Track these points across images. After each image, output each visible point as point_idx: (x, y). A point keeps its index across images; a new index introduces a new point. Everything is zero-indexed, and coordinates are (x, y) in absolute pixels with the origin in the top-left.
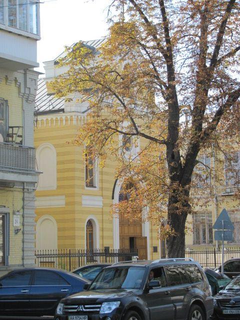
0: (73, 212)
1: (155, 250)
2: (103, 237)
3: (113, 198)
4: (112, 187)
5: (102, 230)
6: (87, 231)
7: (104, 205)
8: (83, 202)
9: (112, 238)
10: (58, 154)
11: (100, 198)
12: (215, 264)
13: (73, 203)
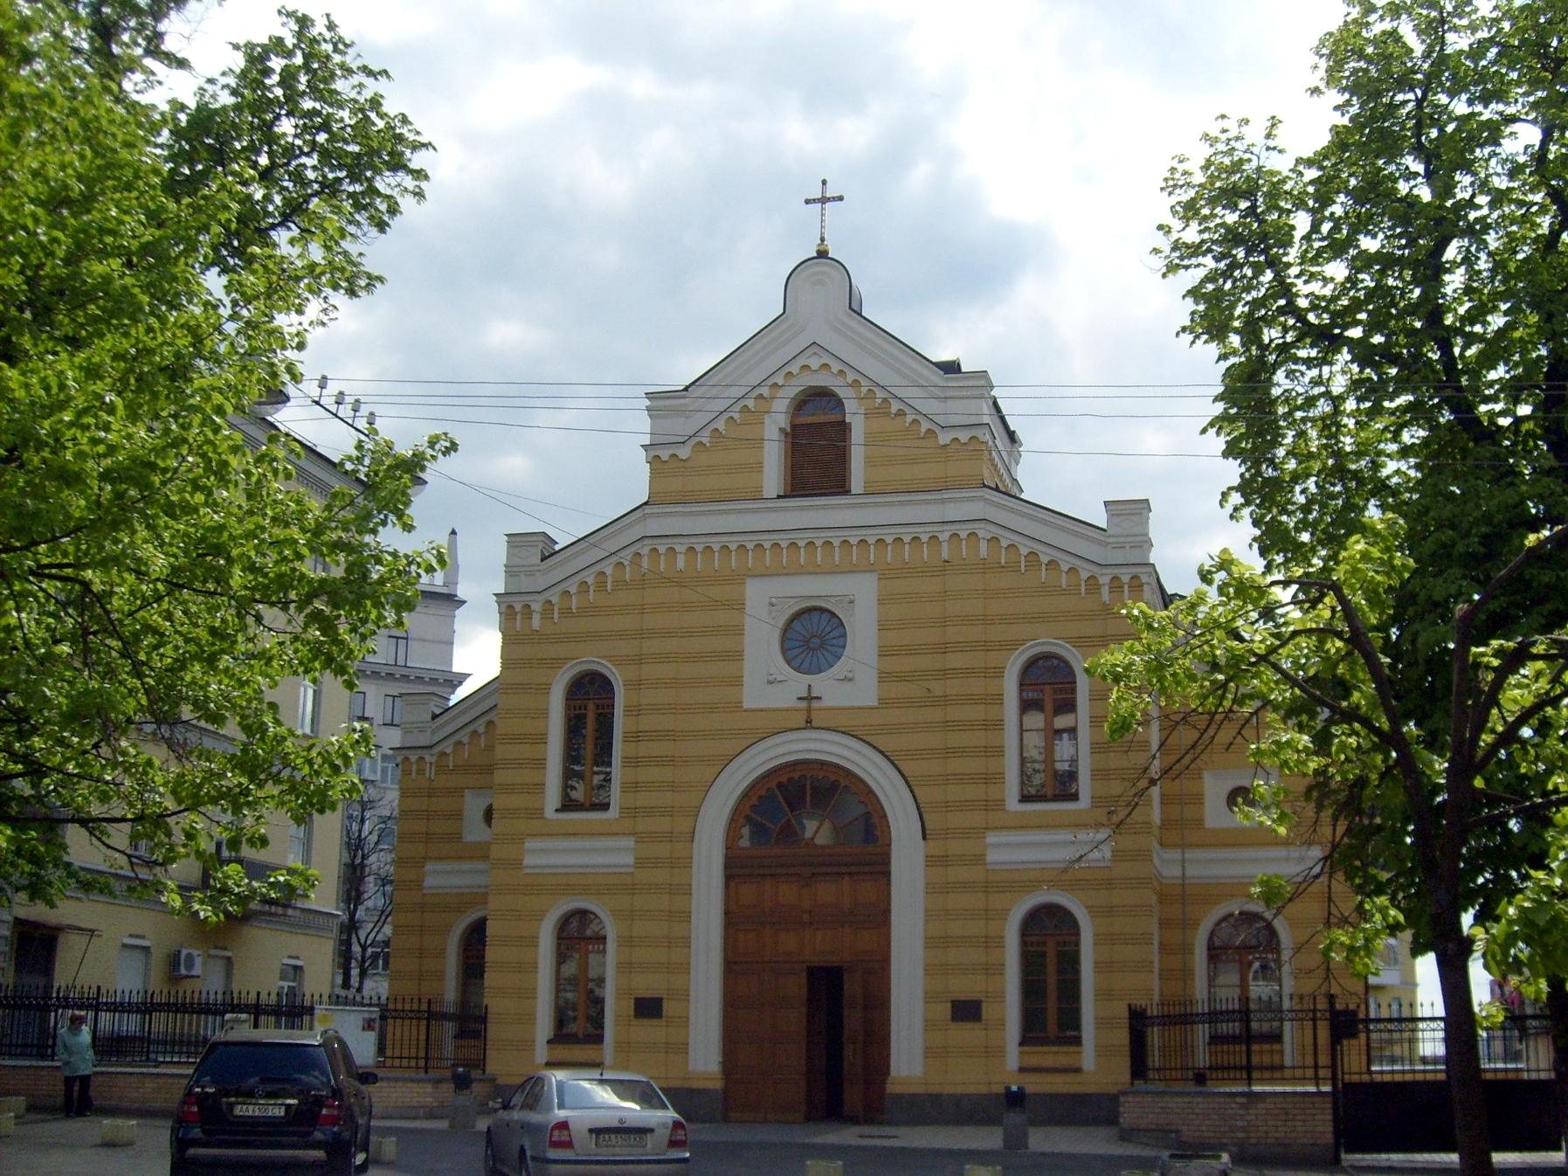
5: (627, 942)
7: (641, 863)
11: (629, 842)
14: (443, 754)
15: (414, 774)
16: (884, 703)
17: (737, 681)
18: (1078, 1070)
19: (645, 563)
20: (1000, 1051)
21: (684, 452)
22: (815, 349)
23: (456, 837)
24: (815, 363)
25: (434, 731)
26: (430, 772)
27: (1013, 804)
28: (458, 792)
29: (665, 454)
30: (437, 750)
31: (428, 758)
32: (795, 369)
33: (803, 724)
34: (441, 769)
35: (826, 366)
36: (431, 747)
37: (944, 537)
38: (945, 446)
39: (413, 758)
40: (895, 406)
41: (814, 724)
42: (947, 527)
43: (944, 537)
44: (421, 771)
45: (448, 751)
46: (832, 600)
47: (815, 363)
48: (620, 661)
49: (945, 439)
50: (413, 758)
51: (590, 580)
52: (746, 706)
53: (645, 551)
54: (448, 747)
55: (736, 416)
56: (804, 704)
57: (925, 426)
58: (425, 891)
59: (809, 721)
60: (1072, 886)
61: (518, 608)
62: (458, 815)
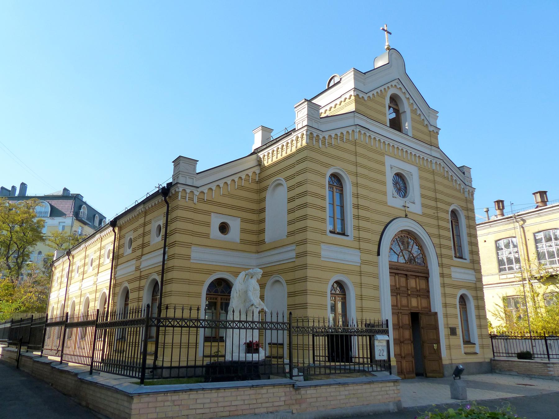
0: (304, 267)
1: (453, 331)
2: (361, 309)
3: (379, 254)
4: (378, 240)
7: (364, 262)
8: (323, 253)
9: (379, 311)
10: (290, 189)
11: (357, 252)
13: (304, 254)
14: (202, 192)
15: (187, 198)
16: (424, 215)
17: (385, 193)
18: (476, 353)
19: (357, 136)
20: (459, 346)
21: (366, 98)
22: (397, 81)
23: (207, 236)
24: (398, 87)
27: (454, 258)
28: (208, 213)
29: (361, 95)
30: (200, 190)
31: (197, 193)
32: (394, 83)
33: (405, 216)
35: (400, 88)
36: (198, 187)
37: (434, 161)
38: (430, 132)
40: (419, 112)
41: (408, 216)
42: (435, 159)
43: (434, 161)
44: (191, 199)
45: (206, 191)
46: (406, 172)
47: (398, 87)
48: (350, 173)
49: (431, 129)
50: (188, 191)
51: (339, 134)
52: (389, 204)
53: (358, 130)
54: (205, 189)
55: (379, 93)
56: (403, 208)
57: (426, 123)
59: (406, 215)
60: (468, 288)
61: (315, 135)
62: (208, 224)
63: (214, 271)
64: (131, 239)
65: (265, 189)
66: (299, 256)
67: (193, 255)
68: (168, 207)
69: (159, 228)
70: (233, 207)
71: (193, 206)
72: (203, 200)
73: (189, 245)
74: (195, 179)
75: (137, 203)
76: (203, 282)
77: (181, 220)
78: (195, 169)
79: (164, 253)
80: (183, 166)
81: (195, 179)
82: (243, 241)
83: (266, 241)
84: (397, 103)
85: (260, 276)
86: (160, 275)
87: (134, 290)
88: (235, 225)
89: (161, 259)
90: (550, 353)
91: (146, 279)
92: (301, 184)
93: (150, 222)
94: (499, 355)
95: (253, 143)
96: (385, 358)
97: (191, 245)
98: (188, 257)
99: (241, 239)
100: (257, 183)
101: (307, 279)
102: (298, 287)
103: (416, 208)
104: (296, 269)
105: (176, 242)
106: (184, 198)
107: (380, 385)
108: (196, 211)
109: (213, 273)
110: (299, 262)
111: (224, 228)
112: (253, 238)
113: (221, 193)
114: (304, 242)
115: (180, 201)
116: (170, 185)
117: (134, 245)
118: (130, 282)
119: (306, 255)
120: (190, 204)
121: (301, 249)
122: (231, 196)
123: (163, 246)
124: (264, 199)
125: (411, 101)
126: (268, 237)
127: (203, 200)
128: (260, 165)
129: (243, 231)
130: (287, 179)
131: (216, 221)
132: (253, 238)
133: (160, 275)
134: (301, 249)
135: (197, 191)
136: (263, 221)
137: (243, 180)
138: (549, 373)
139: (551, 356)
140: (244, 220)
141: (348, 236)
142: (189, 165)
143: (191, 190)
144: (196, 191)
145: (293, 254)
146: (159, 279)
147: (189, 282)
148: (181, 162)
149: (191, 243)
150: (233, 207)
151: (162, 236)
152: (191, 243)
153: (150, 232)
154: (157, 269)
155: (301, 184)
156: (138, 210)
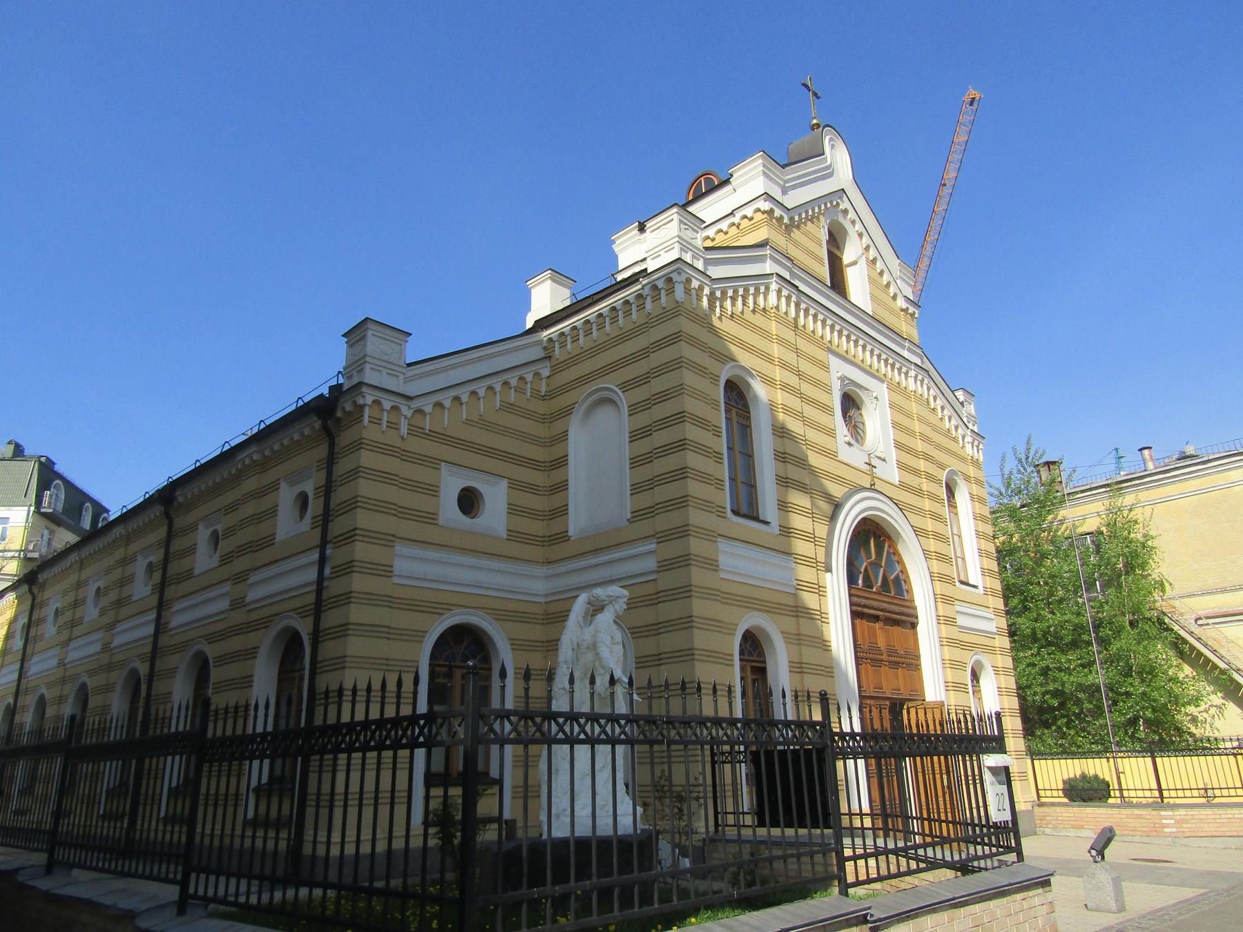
0: (685, 592)
6: (742, 669)
10: (634, 409)
12: (1160, 790)
13: (684, 561)
14: (419, 411)
15: (385, 424)
17: (831, 433)
23: (430, 518)
25: (407, 380)
26: (404, 430)
27: (957, 584)
28: (433, 463)
29: (778, 213)
30: (416, 404)
31: (405, 411)
34: (417, 431)
36: (409, 398)
39: (387, 405)
44: (394, 426)
45: (428, 409)
50: (387, 405)
52: (840, 458)
58: (395, 580)
63: (449, 607)
64: (215, 533)
65: (567, 412)
66: (665, 566)
67: (400, 566)
68: (332, 445)
69: (303, 500)
70: (491, 452)
71: (398, 443)
72: (422, 431)
73: (389, 540)
74: (402, 376)
75: (227, 447)
76: (423, 633)
77: (370, 477)
78: (401, 353)
79: (322, 561)
80: (374, 344)
81: (402, 376)
82: (514, 535)
83: (570, 534)
84: (837, 243)
85: (621, 606)
86: (311, 615)
87: (224, 659)
88: (496, 496)
89: (312, 575)
90: (1164, 786)
91: (264, 630)
92: (665, 395)
93: (274, 487)
94: (1173, 794)
95: (528, 308)
96: (1007, 816)
97: (394, 539)
98: (386, 571)
99: (508, 530)
100: (543, 398)
101: (692, 621)
102: (669, 642)
103: (890, 473)
104: (659, 600)
105: (358, 532)
106: (376, 421)
107: (1019, 896)
108: (404, 455)
109: (446, 611)
110: (667, 581)
111: (469, 501)
112: (538, 528)
113: (464, 417)
114: (682, 532)
115: (369, 431)
116: (336, 390)
117: (225, 546)
118: (211, 638)
119: (688, 562)
120: (391, 438)
121: (672, 549)
122: (484, 424)
123: (318, 542)
124: (565, 435)
125: (866, 240)
126: (578, 521)
127: (422, 431)
128: (550, 357)
129: (513, 510)
130: (626, 386)
131: (452, 484)
132: (538, 528)
133: (311, 615)
134: (672, 549)
135: (409, 408)
136: (563, 487)
137: (513, 390)
138: (1166, 830)
139: (1165, 794)
140: (515, 485)
141: (767, 523)
142: (389, 343)
143: (393, 404)
144: (407, 407)
145: (650, 564)
146: (304, 628)
147: (387, 633)
148: (370, 333)
149: (394, 536)
150: (491, 452)
151: (314, 518)
152: (394, 536)
153: (273, 511)
154: (298, 603)
155: (665, 395)
156: (241, 457)
